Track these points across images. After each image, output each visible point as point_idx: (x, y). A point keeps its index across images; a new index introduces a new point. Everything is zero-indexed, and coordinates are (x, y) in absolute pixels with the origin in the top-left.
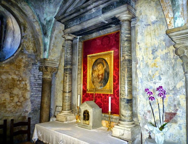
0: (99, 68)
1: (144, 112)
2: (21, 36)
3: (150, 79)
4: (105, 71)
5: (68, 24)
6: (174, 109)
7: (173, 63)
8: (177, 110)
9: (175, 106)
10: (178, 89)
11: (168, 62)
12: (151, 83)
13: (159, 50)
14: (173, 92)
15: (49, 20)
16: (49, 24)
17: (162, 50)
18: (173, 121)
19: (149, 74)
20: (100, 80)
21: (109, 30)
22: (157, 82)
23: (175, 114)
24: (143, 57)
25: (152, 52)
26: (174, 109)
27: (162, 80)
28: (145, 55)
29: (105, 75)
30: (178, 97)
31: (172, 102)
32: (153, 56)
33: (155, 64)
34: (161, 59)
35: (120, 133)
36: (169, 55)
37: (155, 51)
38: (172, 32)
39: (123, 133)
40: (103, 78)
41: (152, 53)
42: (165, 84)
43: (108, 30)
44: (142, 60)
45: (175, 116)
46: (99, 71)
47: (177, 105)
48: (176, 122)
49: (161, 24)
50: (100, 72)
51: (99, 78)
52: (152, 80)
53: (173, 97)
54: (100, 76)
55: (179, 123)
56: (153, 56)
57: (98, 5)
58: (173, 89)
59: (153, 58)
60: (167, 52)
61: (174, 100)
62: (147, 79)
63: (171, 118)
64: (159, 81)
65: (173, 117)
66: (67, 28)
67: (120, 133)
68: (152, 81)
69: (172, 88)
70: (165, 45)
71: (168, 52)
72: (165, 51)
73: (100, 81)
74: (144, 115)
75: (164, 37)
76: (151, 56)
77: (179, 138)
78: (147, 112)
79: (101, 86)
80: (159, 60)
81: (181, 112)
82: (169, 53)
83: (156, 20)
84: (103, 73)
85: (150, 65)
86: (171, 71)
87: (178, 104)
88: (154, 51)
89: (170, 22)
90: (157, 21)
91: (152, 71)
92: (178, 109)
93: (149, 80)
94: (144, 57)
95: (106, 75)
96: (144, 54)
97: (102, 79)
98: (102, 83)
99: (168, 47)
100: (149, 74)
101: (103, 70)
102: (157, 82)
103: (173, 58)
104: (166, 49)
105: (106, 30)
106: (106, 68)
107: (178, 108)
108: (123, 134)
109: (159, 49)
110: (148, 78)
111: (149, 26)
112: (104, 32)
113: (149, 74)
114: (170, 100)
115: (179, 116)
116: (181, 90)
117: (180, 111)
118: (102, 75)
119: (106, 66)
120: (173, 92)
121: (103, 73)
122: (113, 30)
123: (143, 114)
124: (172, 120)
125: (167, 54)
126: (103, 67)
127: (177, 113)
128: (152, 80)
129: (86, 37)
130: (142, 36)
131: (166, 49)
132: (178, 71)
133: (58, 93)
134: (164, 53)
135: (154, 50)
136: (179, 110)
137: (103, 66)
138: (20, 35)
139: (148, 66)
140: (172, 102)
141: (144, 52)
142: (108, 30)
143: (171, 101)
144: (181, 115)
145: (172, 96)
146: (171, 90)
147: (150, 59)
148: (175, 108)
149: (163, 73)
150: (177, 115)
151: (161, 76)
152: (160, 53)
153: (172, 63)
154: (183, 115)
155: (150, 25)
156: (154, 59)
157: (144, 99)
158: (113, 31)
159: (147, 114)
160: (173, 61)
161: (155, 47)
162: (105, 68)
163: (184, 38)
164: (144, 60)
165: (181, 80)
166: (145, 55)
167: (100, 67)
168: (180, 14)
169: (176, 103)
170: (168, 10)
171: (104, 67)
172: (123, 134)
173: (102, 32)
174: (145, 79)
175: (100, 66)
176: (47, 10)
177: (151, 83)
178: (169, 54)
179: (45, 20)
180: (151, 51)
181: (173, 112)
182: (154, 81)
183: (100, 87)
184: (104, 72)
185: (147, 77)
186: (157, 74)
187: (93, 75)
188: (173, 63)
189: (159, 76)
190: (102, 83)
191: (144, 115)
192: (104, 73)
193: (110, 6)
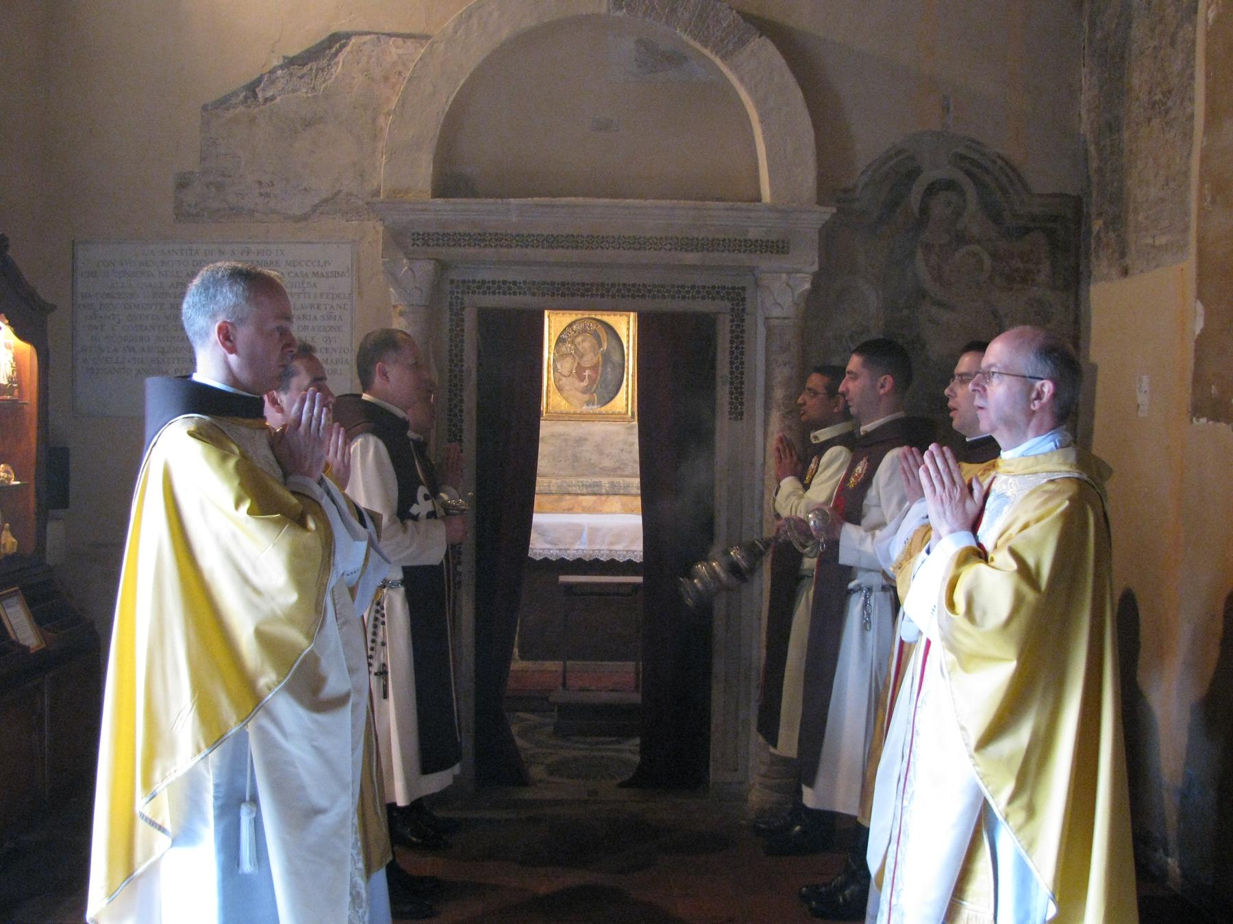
0: (580, 347)
4: (606, 357)
20: (585, 384)
46: (582, 356)
51: (582, 379)
54: (587, 373)
73: (587, 386)
79: (588, 403)
84: (598, 363)
97: (592, 381)
98: (595, 392)
118: (594, 368)
121: (598, 363)
126: (597, 347)
162: (605, 348)
167: (586, 345)
171: (600, 345)
175: (583, 341)
183: (587, 405)
184: (600, 359)
187: (559, 366)
190: (595, 392)
192: (601, 363)
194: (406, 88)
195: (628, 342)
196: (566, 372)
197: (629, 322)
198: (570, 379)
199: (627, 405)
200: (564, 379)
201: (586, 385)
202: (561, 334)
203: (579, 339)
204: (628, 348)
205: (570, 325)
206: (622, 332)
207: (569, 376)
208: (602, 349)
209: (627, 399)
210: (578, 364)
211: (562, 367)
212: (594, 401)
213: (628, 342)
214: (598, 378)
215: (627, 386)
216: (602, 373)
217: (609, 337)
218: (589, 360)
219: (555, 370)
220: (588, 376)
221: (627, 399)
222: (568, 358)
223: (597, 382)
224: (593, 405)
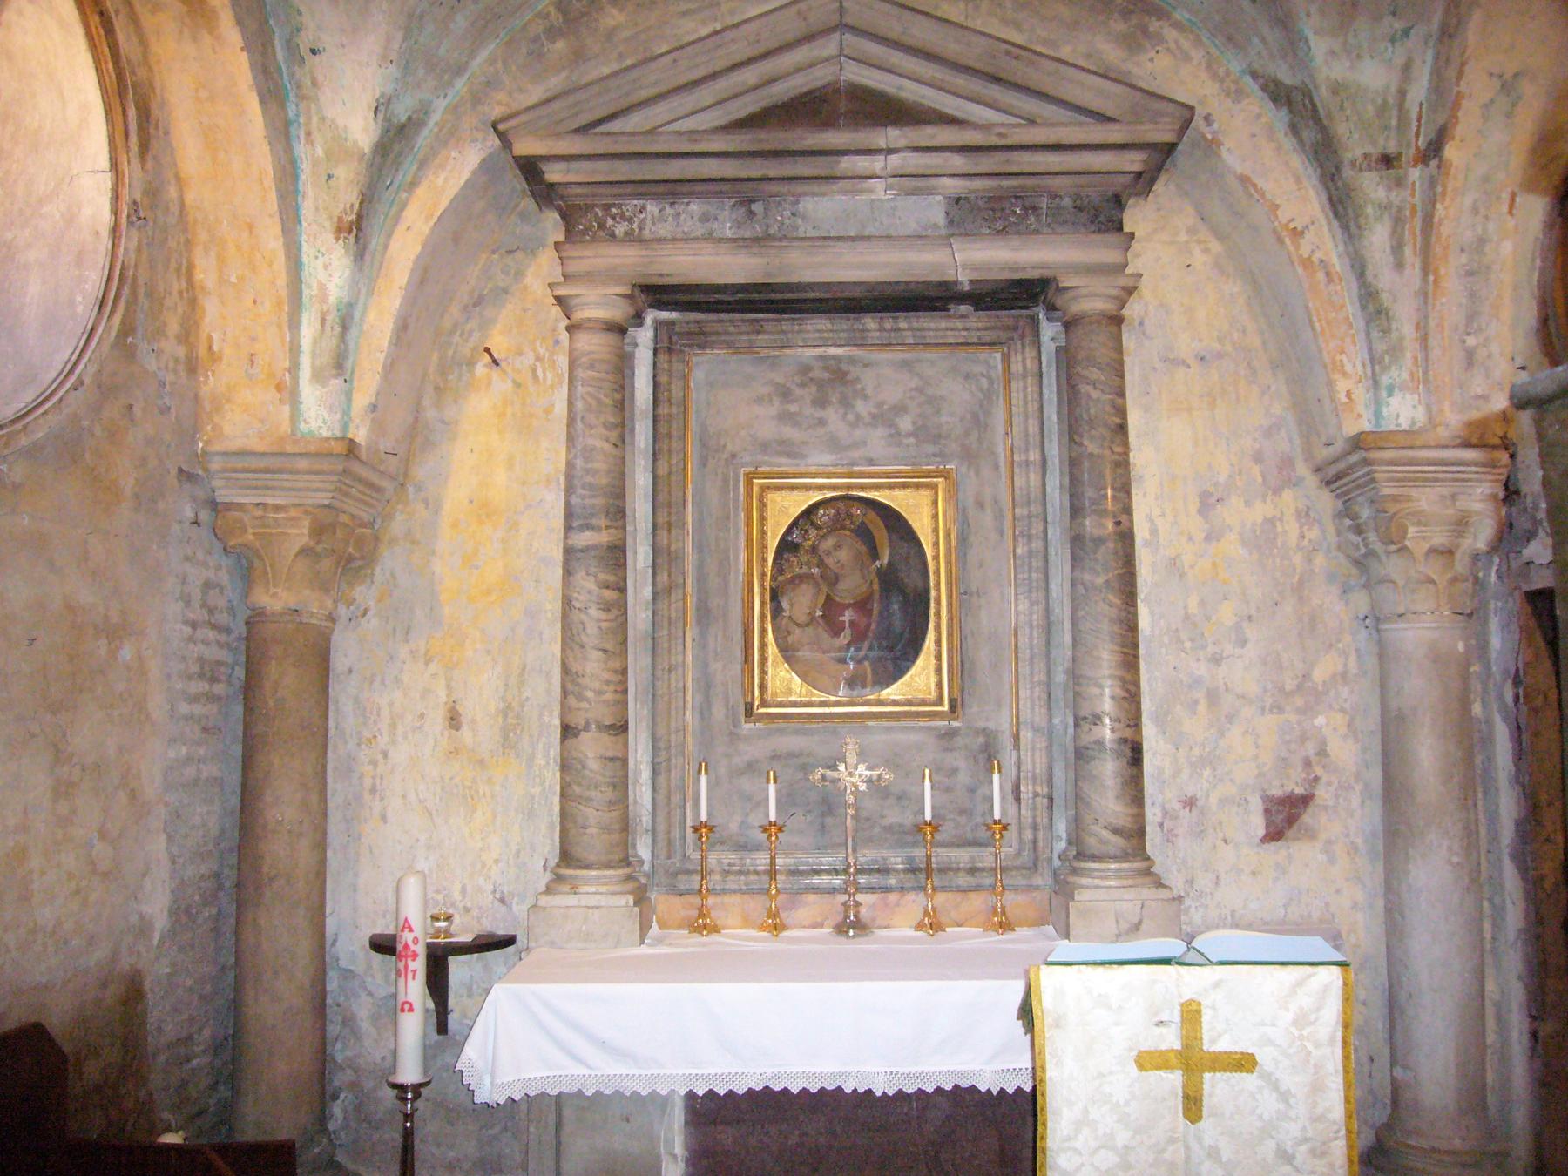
0: (829, 561)
1: (1164, 808)
2: (116, 197)
3: (1192, 640)
4: (889, 581)
5: (607, 207)
6: (1304, 776)
7: (1298, 571)
8: (1317, 779)
9: (1307, 763)
10: (1320, 688)
11: (1278, 560)
12: (1198, 660)
13: (1236, 501)
14: (1299, 701)
15: (404, 119)
16: (397, 147)
17: (1248, 503)
18: (1299, 830)
19: (1187, 617)
21: (937, 330)
22: (1228, 657)
23: (1305, 800)
24: (1152, 522)
25: (1198, 504)
26: (1304, 776)
27: (1249, 646)
28: (1163, 515)
29: (886, 607)
30: (1320, 721)
31: (1293, 746)
32: (1206, 526)
33: (1214, 565)
34: (1244, 543)
35: (1121, 921)
36: (1279, 529)
37: (1213, 500)
38: (1381, 444)
39: (1136, 920)
40: (869, 625)
41: (1200, 512)
42: (1265, 663)
43: (932, 325)
44: (1148, 536)
45: (1310, 810)
46: (834, 581)
47: (1314, 759)
48: (1311, 835)
49: (1242, 372)
50: (842, 586)
51: (836, 630)
52: (1204, 647)
53: (1299, 723)
54: (848, 616)
55: (1323, 836)
56: (1206, 526)
57: (928, 172)
58: (1299, 687)
59: (1203, 535)
60: (1269, 516)
61: (1303, 739)
62: (1179, 640)
63: (1291, 820)
64: (1238, 651)
65: (1299, 815)
66: (594, 239)
67: (1117, 922)
68: (1201, 654)
69: (1295, 682)
70: (1260, 480)
71: (1274, 517)
72: (1260, 511)
74: (1161, 825)
75: (1255, 440)
76: (1196, 525)
77: (1327, 904)
78: (1177, 806)
80: (1231, 546)
81: (1332, 789)
82: (1281, 520)
83: (1216, 346)
85: (1192, 567)
86: (1288, 607)
87: (1318, 754)
88: (1208, 502)
89: (1348, 394)
90: (1220, 355)
91: (1202, 603)
92: (1319, 774)
93: (1188, 644)
94: (1159, 522)
95: (896, 607)
96: (1157, 512)
99: (1277, 491)
100: (1187, 617)
101: (873, 576)
102: (1228, 657)
103: (1298, 546)
104: (1265, 501)
105: (915, 325)
106: (890, 563)
107: (1318, 771)
108: (1140, 923)
109: (1234, 499)
110: (1184, 636)
111: (1181, 372)
112: (899, 330)
113: (1186, 613)
114: (1287, 737)
115: (1326, 808)
116: (1332, 693)
117: (1329, 784)
118: (862, 605)
119: (892, 547)
120: (1299, 701)
121: (872, 594)
122: (965, 333)
123: (1158, 819)
124: (1295, 827)
125: (1270, 522)
127: (1317, 793)
128: (1204, 647)
129: (732, 329)
130: (1146, 411)
131: (1265, 501)
132: (1321, 606)
133: (394, 742)
134: (1260, 520)
135: (1212, 494)
136: (1324, 780)
137: (864, 549)
138: (106, 181)
139: (1182, 575)
140: (1293, 746)
141: (1156, 499)
142: (932, 325)
143: (1289, 742)
144: (1331, 803)
145: (1293, 718)
146: (1291, 693)
147: (1190, 539)
148: (1308, 774)
149: (1253, 612)
150: (1318, 801)
151: (1245, 624)
152: (1241, 514)
153: (1295, 569)
154: (1337, 796)
155: (1189, 367)
156: (1208, 539)
157: (1161, 742)
158: (961, 341)
159: (1177, 818)
160: (1298, 559)
161: (1216, 484)
162: (886, 561)
163: (1399, 480)
164: (1161, 540)
165: (1331, 645)
166: (1163, 515)
167: (844, 555)
168: (1405, 376)
169: (1310, 749)
170: (1342, 340)
171: (875, 555)
172: (1140, 923)
173: (882, 330)
174: (1166, 639)
175: (838, 547)
176: (422, 40)
177: (1198, 660)
178: (1278, 524)
179: (381, 116)
180: (1197, 500)
181: (1299, 790)
182: (1211, 649)
184: (876, 587)
185: (1177, 630)
186: (1227, 614)
187: (785, 604)
188: (1298, 571)
189: (1238, 628)
191: (1161, 825)
192: (877, 596)
193: (1006, 205)
194: (472, 55)
195: (936, 544)
196: (803, 619)
197: (935, 503)
198: (810, 630)
199: (939, 685)
200: (798, 631)
201: (846, 642)
202: (789, 531)
203: (829, 543)
204: (936, 558)
205: (809, 512)
206: (921, 524)
207: (807, 625)
208: (878, 563)
209: (938, 671)
210: (828, 596)
211: (792, 605)
212: (865, 677)
213: (936, 544)
214: (873, 626)
215: (938, 642)
216: (881, 614)
217: (894, 538)
218: (852, 585)
219: (777, 611)
220: (852, 623)
221: (938, 671)
222: (804, 586)
223: (871, 635)
224: (864, 686)
